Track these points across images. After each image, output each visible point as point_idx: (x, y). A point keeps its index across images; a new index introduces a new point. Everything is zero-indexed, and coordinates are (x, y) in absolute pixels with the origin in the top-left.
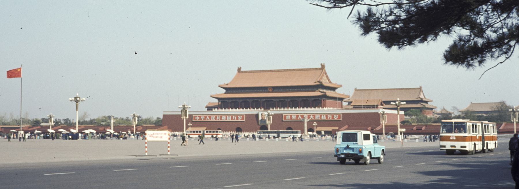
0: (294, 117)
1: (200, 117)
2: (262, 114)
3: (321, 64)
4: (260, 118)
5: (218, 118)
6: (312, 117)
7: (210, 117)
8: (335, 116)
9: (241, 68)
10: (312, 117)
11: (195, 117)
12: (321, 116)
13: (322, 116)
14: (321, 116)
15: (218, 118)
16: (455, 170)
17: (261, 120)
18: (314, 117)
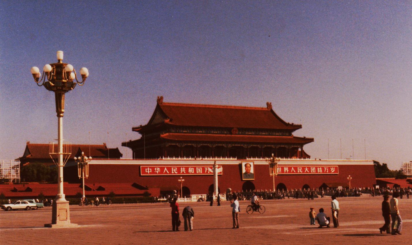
0: (286, 169)
1: (153, 169)
2: (246, 165)
3: (267, 104)
4: (244, 171)
5: (183, 170)
6: (306, 169)
7: (169, 169)
8: (332, 169)
9: (162, 98)
10: (306, 169)
11: (144, 169)
12: (316, 168)
13: (318, 169)
14: (316, 168)
15: (183, 170)
16: (78, 228)
17: (246, 173)
18: (309, 170)
